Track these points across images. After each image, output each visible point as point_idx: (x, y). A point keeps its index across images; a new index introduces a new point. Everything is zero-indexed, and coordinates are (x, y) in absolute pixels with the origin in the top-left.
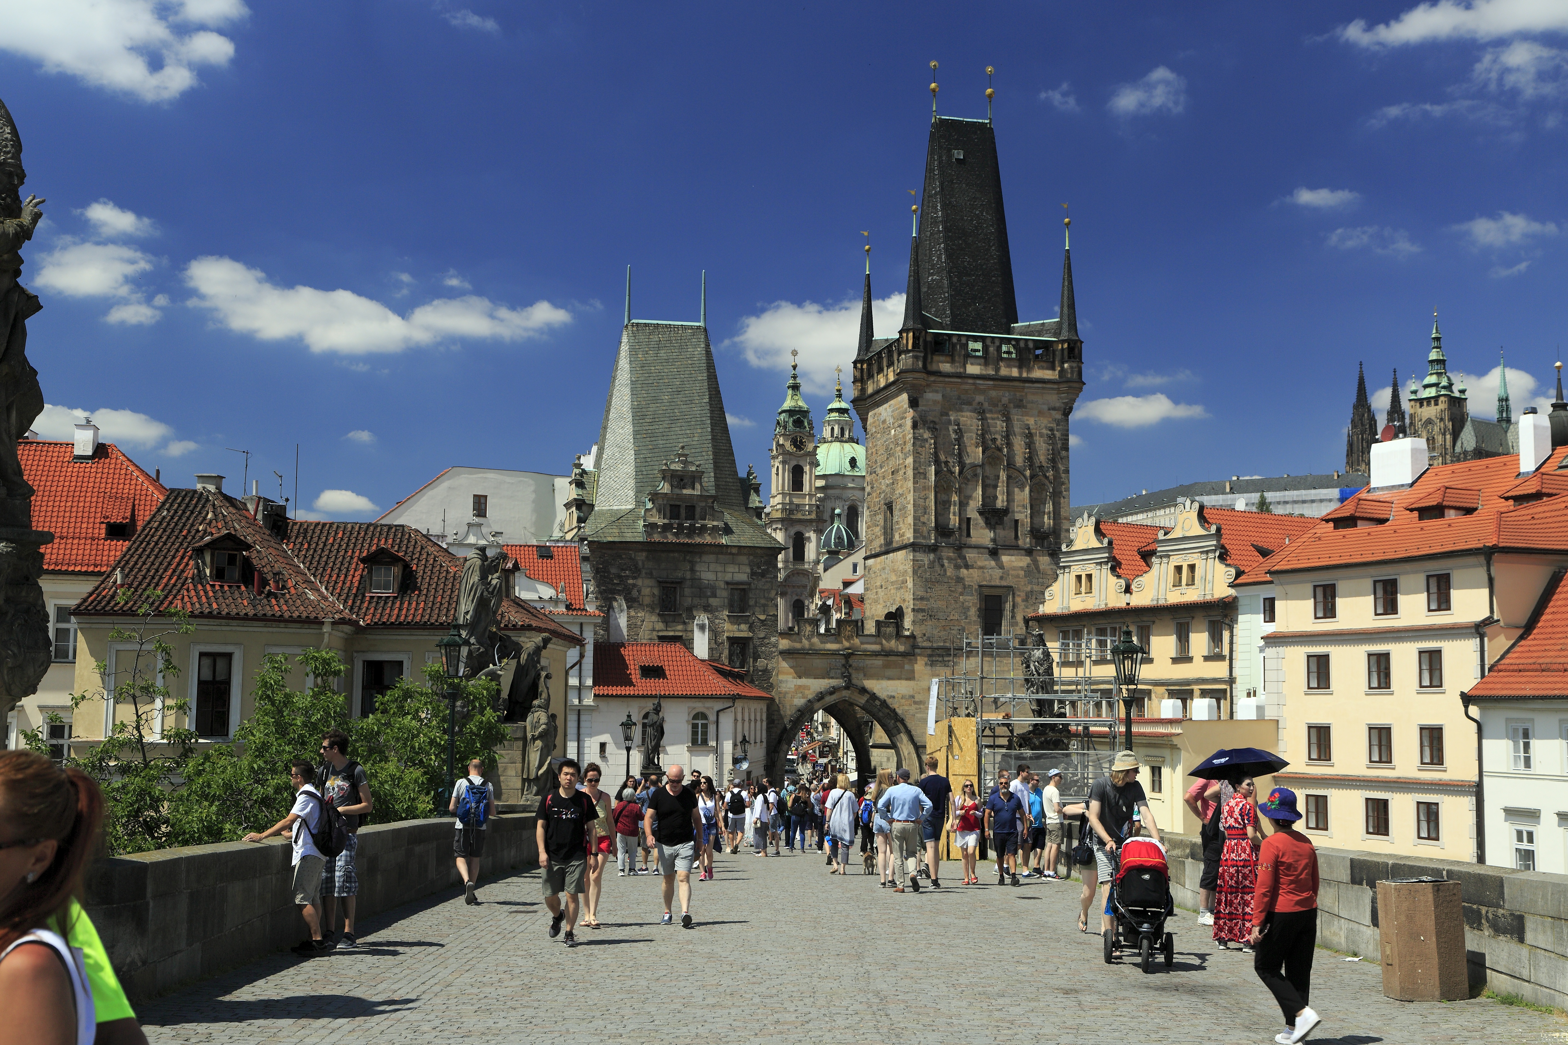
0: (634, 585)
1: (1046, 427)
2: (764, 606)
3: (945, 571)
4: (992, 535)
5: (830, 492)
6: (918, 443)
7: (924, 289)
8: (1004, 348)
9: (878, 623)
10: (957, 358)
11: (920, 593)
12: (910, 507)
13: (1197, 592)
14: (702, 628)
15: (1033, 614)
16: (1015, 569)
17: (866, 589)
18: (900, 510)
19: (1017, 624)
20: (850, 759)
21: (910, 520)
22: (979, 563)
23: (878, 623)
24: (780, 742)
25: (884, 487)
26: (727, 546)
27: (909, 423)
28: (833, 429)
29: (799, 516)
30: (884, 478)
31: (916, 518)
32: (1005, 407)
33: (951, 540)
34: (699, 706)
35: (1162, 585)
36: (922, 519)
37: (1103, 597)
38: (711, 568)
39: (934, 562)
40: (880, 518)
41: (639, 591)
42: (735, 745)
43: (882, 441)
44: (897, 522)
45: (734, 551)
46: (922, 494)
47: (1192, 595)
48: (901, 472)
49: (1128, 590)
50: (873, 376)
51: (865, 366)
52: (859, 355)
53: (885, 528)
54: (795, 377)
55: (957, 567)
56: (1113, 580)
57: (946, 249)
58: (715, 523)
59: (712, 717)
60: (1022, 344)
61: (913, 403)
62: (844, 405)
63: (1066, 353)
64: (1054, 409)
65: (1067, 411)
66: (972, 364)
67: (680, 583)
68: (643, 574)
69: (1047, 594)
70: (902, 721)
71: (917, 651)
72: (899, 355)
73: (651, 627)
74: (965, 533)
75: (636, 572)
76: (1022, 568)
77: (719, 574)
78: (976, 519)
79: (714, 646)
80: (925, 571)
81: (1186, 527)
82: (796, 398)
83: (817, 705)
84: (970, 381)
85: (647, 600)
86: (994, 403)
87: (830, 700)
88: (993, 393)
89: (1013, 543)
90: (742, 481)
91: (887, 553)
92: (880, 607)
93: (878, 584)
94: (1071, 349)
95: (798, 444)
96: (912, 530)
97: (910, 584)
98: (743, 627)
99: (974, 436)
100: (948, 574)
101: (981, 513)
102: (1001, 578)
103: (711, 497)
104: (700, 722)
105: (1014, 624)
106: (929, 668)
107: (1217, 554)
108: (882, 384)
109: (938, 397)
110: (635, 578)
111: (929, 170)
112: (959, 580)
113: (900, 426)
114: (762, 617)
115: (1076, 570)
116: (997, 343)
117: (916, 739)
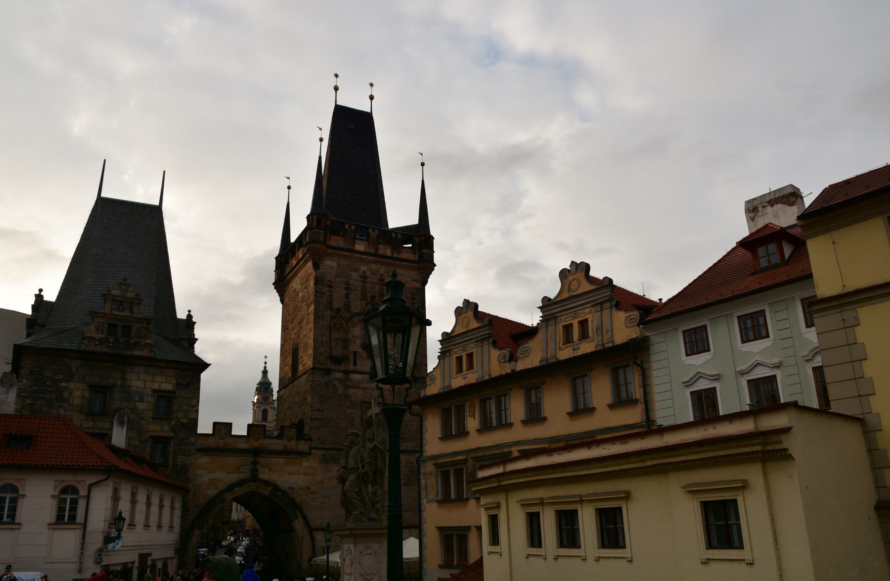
0: (67, 388)
9: (282, 428)
12: (311, 342)
13: (595, 343)
14: (121, 423)
21: (311, 351)
27: (312, 282)
30: (293, 329)
31: (315, 349)
32: (382, 275)
33: (342, 367)
34: (68, 479)
35: (551, 346)
37: (486, 370)
40: (289, 360)
41: (71, 393)
45: (162, 365)
47: (587, 348)
48: (305, 320)
49: (512, 358)
50: (288, 263)
54: (265, 368)
55: (346, 387)
56: (495, 354)
58: (148, 341)
59: (83, 492)
61: (316, 266)
64: (415, 281)
70: (299, 508)
71: (314, 451)
74: (352, 363)
77: (148, 383)
79: (137, 443)
81: (573, 287)
83: (228, 496)
84: (358, 255)
85: (77, 402)
87: (239, 491)
88: (374, 266)
91: (293, 381)
98: (166, 428)
100: (339, 392)
104: (69, 497)
107: (614, 303)
108: (294, 262)
109: (334, 264)
110: (67, 381)
114: (184, 421)
116: (377, 232)
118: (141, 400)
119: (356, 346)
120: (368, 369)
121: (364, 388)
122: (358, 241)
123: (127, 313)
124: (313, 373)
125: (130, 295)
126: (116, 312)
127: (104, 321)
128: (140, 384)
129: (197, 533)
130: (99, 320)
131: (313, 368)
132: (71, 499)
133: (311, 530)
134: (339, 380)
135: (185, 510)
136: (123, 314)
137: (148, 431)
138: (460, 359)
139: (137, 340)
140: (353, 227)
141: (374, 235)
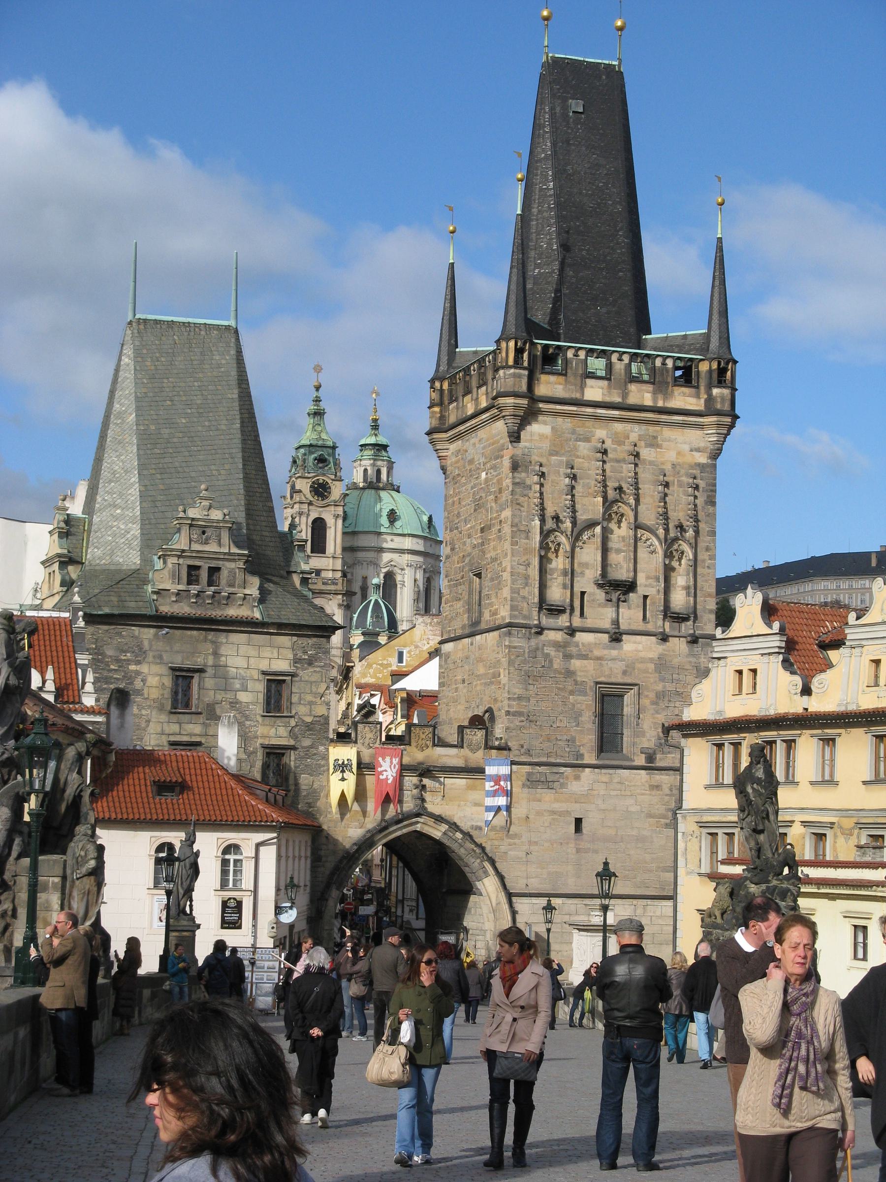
0: (138, 673)
1: (687, 475)
2: (311, 703)
3: (551, 662)
4: (614, 615)
5: (361, 555)
6: (518, 490)
7: (529, 286)
8: (634, 368)
9: (461, 729)
10: (571, 378)
11: (518, 690)
12: (506, 576)
15: (676, 721)
16: (643, 661)
17: (441, 684)
18: (492, 579)
19: (643, 734)
20: (407, 909)
21: (506, 592)
22: (597, 653)
23: (461, 729)
24: (328, 886)
25: (469, 549)
26: (263, 624)
27: (506, 463)
28: (366, 470)
29: (320, 586)
30: (469, 536)
31: (513, 591)
34: (233, 837)
36: (521, 594)
38: (241, 652)
39: (537, 649)
41: (144, 681)
42: (278, 890)
43: (469, 486)
44: (488, 597)
46: (524, 558)
48: (494, 529)
49: (807, 691)
51: (446, 386)
52: (437, 370)
53: (469, 603)
54: (317, 400)
55: (568, 657)
57: (559, 234)
58: (247, 592)
59: (248, 851)
60: (658, 362)
62: (381, 440)
63: (715, 376)
64: (698, 450)
65: (715, 455)
66: (592, 387)
67: (201, 671)
68: (150, 659)
69: (694, 695)
72: (496, 370)
73: (159, 730)
74: (577, 612)
75: (140, 655)
76: (651, 660)
77: (252, 660)
78: (594, 594)
80: (524, 662)
82: (319, 428)
84: (589, 410)
85: (155, 694)
86: (619, 440)
88: (619, 427)
89: (641, 626)
90: (283, 535)
91: (472, 635)
92: (461, 707)
93: (459, 678)
94: (722, 371)
95: (321, 490)
96: (508, 607)
97: (504, 679)
99: (593, 483)
100: (555, 666)
101: (600, 586)
102: (625, 673)
103: (243, 555)
104: (231, 857)
105: (640, 734)
106: (526, 790)
108: (470, 411)
110: (139, 663)
111: (537, 126)
112: (569, 673)
113: (494, 467)
114: (309, 719)
115: (736, 661)
116: (626, 358)
117: (508, 885)
118: (245, 690)
119: (586, 581)
120: (607, 624)
121: (599, 658)
122: (589, 382)
123: (212, 547)
124: (509, 634)
125: (216, 515)
126: (196, 547)
127: (181, 561)
128: (240, 662)
129: (335, 893)
130: (175, 560)
131: (510, 625)
132: (235, 860)
133: (510, 896)
134: (557, 645)
135: (316, 859)
136: (207, 548)
137: (257, 737)
138: (740, 672)
139: (231, 590)
140: (582, 354)
141: (619, 367)
